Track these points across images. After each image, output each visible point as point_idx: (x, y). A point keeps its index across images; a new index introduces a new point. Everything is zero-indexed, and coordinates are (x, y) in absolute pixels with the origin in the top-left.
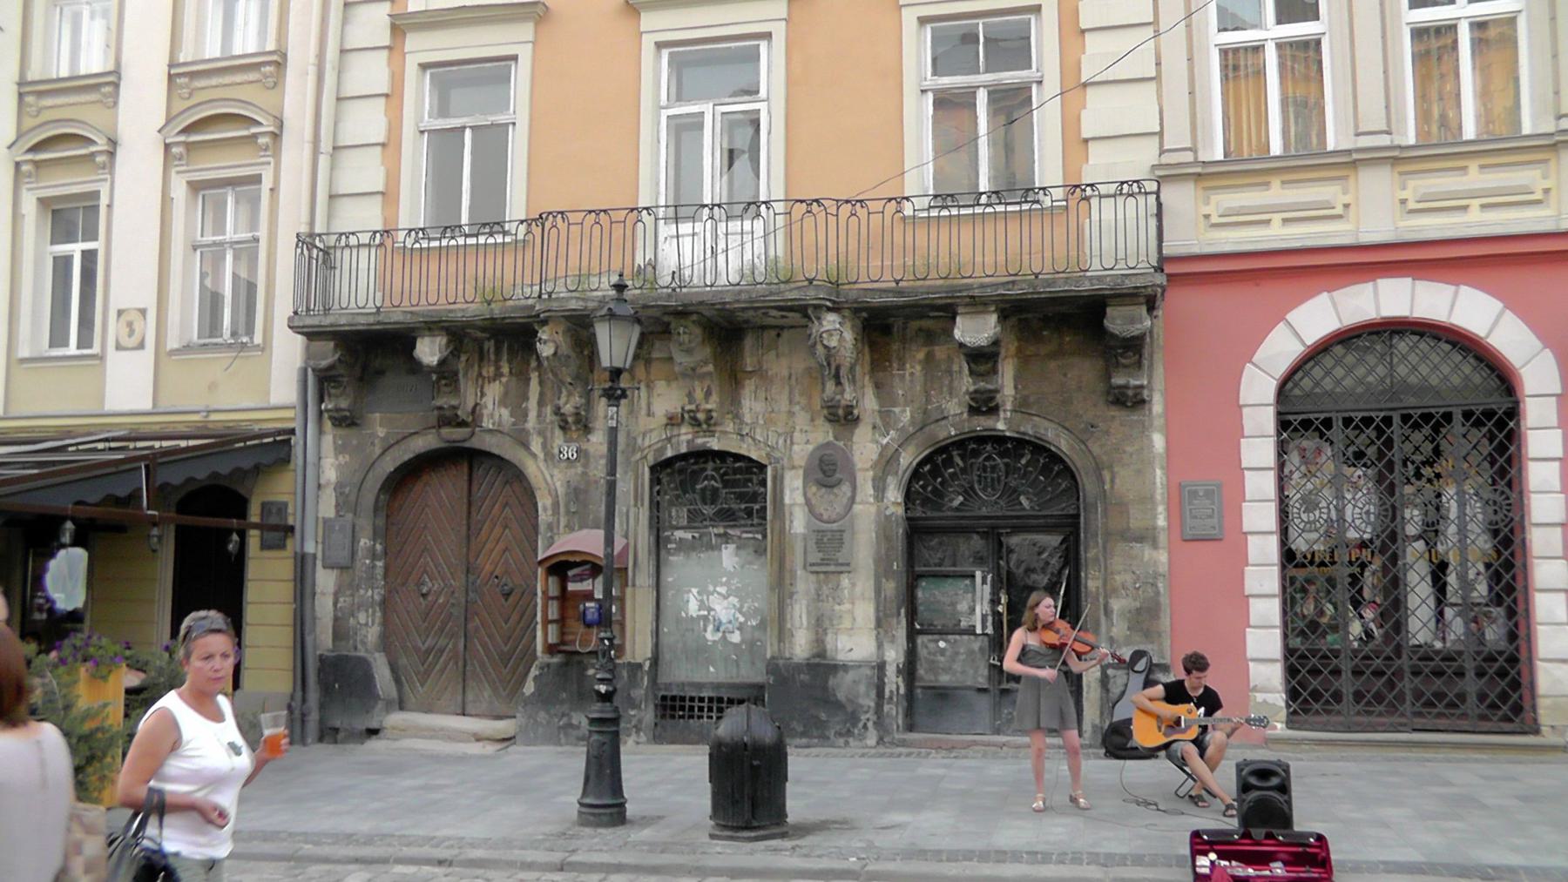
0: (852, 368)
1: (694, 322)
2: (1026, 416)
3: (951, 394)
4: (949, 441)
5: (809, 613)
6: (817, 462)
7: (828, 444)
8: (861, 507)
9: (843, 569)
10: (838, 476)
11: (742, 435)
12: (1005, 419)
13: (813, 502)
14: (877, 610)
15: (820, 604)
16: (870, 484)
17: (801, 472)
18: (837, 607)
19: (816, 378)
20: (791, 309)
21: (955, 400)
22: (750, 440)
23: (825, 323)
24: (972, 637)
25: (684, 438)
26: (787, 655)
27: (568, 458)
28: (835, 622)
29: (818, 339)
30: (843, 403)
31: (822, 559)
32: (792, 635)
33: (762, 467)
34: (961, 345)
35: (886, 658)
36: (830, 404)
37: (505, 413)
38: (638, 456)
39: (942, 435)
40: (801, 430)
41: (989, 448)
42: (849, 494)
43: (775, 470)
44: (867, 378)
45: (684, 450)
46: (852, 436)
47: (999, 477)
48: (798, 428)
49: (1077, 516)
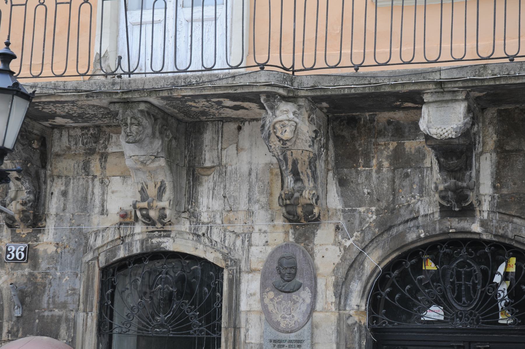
0: (312, 163)
1: (142, 111)
3: (421, 192)
4: (419, 244)
6: (276, 265)
8: (322, 315)
11: (198, 236)
13: (271, 308)
16: (330, 292)
17: (258, 277)
19: (277, 174)
20: (243, 98)
21: (426, 199)
23: (278, 112)
25: (137, 237)
27: (15, 259)
29: (271, 129)
30: (302, 201)
33: (220, 270)
34: (428, 137)
38: (89, 256)
39: (411, 236)
40: (260, 230)
41: (463, 252)
42: (308, 301)
43: (231, 273)
44: (331, 174)
45: (136, 249)
47: (475, 285)
48: (257, 228)
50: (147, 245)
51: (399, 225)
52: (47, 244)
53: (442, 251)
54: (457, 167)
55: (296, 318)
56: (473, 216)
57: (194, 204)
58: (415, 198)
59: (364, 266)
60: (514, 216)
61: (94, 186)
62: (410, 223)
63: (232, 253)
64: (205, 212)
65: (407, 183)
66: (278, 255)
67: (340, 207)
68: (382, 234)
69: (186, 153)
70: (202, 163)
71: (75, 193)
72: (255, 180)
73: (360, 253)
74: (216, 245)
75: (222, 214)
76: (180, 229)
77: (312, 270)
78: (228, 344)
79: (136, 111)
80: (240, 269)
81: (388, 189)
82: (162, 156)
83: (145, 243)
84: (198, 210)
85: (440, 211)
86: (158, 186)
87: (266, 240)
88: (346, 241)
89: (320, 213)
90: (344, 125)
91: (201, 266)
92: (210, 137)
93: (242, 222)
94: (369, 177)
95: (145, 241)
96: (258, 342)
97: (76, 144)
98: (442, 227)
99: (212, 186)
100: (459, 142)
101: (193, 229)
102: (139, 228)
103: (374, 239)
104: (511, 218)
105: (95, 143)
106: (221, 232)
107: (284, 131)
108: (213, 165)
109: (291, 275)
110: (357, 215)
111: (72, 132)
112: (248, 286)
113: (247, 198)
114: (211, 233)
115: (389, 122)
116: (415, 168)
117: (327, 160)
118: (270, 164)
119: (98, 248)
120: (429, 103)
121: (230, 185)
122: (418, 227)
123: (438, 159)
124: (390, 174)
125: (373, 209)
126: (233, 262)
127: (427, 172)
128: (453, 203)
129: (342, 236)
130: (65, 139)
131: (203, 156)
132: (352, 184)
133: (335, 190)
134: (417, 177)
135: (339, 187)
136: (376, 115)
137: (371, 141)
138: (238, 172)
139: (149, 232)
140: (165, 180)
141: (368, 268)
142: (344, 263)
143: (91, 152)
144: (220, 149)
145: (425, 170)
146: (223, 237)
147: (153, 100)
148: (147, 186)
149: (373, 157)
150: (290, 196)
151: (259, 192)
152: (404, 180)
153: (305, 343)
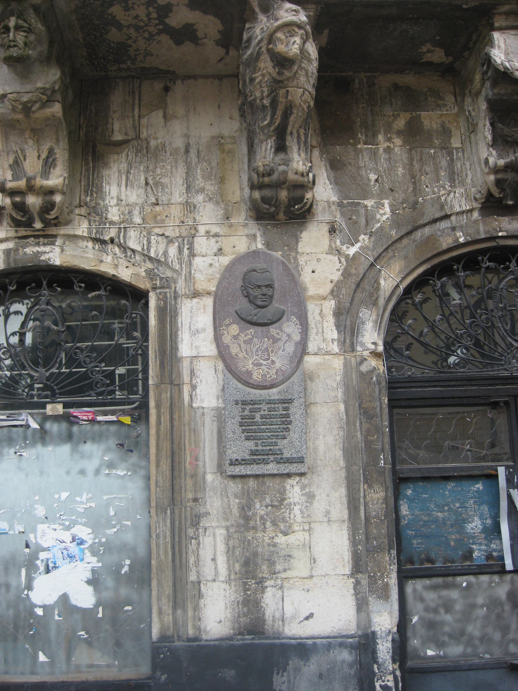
3: (452, 180)
5: (230, 551)
6: (239, 283)
7: (256, 253)
8: (317, 359)
9: (293, 468)
11: (103, 242)
13: (234, 350)
14: (354, 542)
15: (250, 535)
16: (330, 322)
17: (209, 301)
18: (281, 539)
21: (460, 190)
22: (117, 250)
24: (496, 578)
26: (191, 632)
28: (278, 567)
31: (253, 453)
32: (200, 595)
35: (376, 628)
39: (446, 242)
40: (207, 232)
42: (297, 337)
43: (163, 299)
46: (297, 242)
48: (202, 230)
50: (17, 257)
51: (424, 225)
55: (278, 365)
57: (95, 195)
58: (444, 188)
62: (440, 224)
64: (115, 206)
66: (243, 269)
67: (334, 198)
69: (82, 121)
70: (109, 136)
72: (196, 160)
74: (133, 256)
75: (143, 208)
78: (162, 410)
80: (175, 292)
81: (404, 175)
83: (12, 254)
84: (102, 204)
87: (220, 247)
88: (348, 248)
91: (106, 290)
95: (12, 251)
96: (213, 406)
98: (487, 229)
99: (125, 169)
101: (94, 231)
106: (142, 236)
107: (292, 43)
108: (125, 138)
109: (267, 297)
110: (362, 211)
112: (191, 317)
113: (183, 185)
114: (125, 238)
118: (219, 137)
122: (454, 229)
123: (492, 124)
124: (405, 156)
126: (164, 280)
127: (457, 155)
129: (340, 241)
131: (110, 126)
132: (349, 167)
134: (445, 160)
135: (330, 171)
138: (167, 149)
142: (348, 279)
145: (454, 152)
146: (145, 243)
151: (203, 177)
153: (296, 403)
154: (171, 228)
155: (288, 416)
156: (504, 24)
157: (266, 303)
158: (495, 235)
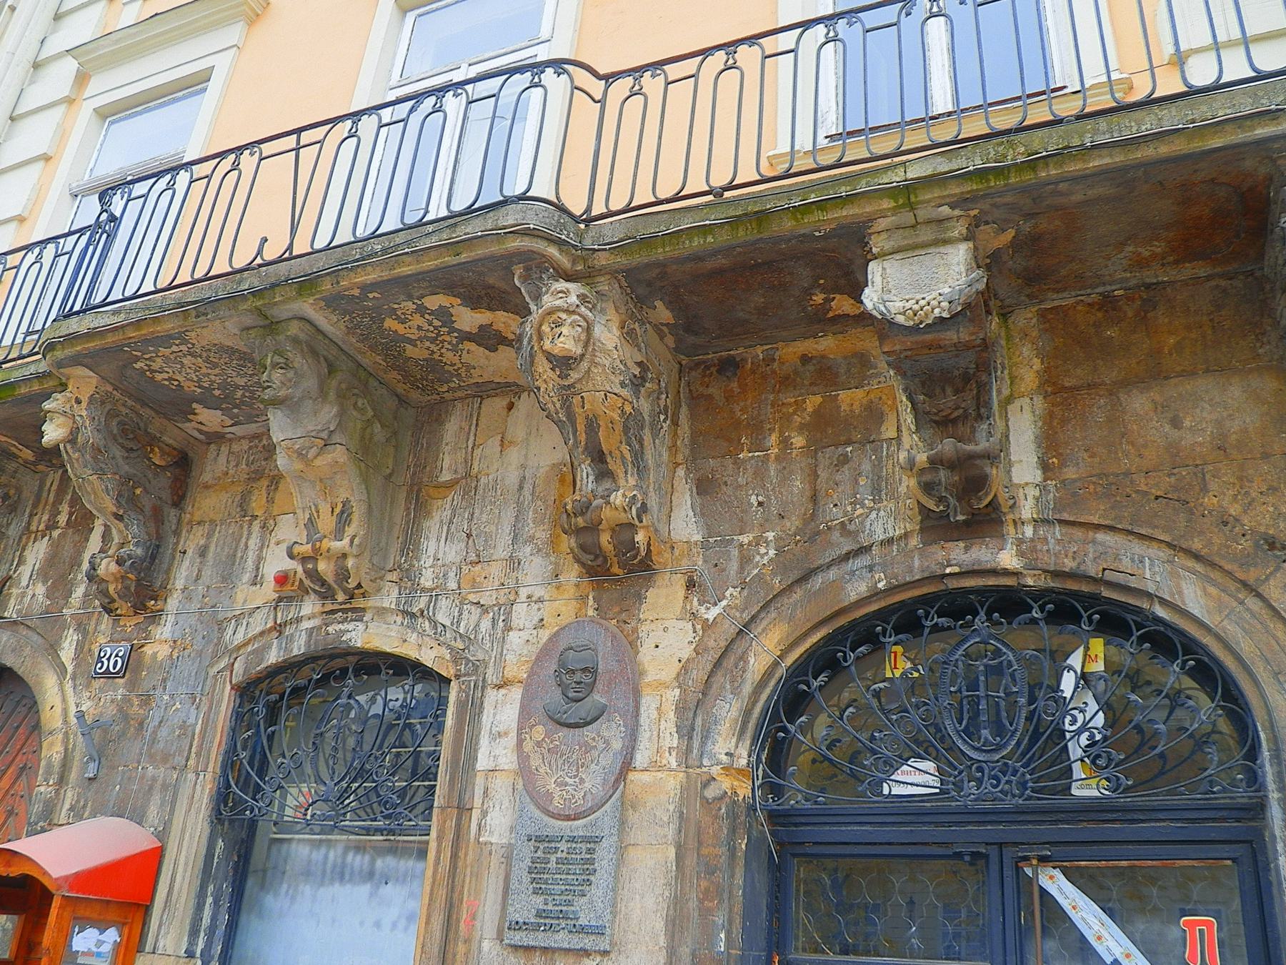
1: (295, 341)
2: (1078, 533)
3: (876, 491)
8: (646, 777)
9: (587, 942)
10: (598, 697)
11: (413, 615)
12: (1020, 542)
13: (535, 762)
16: (669, 723)
17: (516, 694)
31: (539, 914)
36: (580, 521)
37: (40, 589)
39: (857, 589)
40: (529, 597)
44: (681, 472)
48: (523, 593)
49: (1258, 809)
51: (829, 566)
52: (161, 642)
53: (928, 623)
54: (956, 409)
55: (587, 785)
56: (1000, 523)
57: (411, 554)
59: (746, 662)
60: (1098, 527)
61: (250, 534)
63: (471, 648)
65: (845, 474)
68: (789, 589)
71: (219, 550)
73: (738, 633)
76: (379, 604)
77: (630, 676)
79: (281, 338)
82: (339, 441)
85: (922, 530)
86: (337, 510)
89: (649, 544)
90: (711, 374)
92: (456, 428)
93: (497, 583)
94: (760, 474)
96: (504, 841)
97: (237, 466)
100: (959, 338)
102: (310, 606)
103: (771, 601)
104: (1091, 534)
105: (266, 459)
109: (582, 685)
111: (236, 447)
112: (495, 715)
114: (434, 609)
115: (805, 359)
116: (863, 444)
117: (675, 445)
119: (239, 648)
120: (883, 255)
121: (481, 514)
122: (871, 568)
123: (910, 398)
125: (770, 535)
126: (471, 664)
128: (952, 501)
130: (222, 459)
131: (439, 464)
133: (689, 502)
136: (778, 349)
137: (766, 399)
139: (328, 613)
140: (352, 499)
141: (757, 663)
143: (256, 476)
144: (470, 446)
145: (885, 445)
146: (456, 614)
147: (307, 307)
148: (318, 512)
149: (772, 430)
150: (584, 508)
152: (838, 471)
153: (605, 843)
154: (488, 593)
155: (591, 861)
156: (888, 246)
157: (580, 694)
158: (939, 572)
